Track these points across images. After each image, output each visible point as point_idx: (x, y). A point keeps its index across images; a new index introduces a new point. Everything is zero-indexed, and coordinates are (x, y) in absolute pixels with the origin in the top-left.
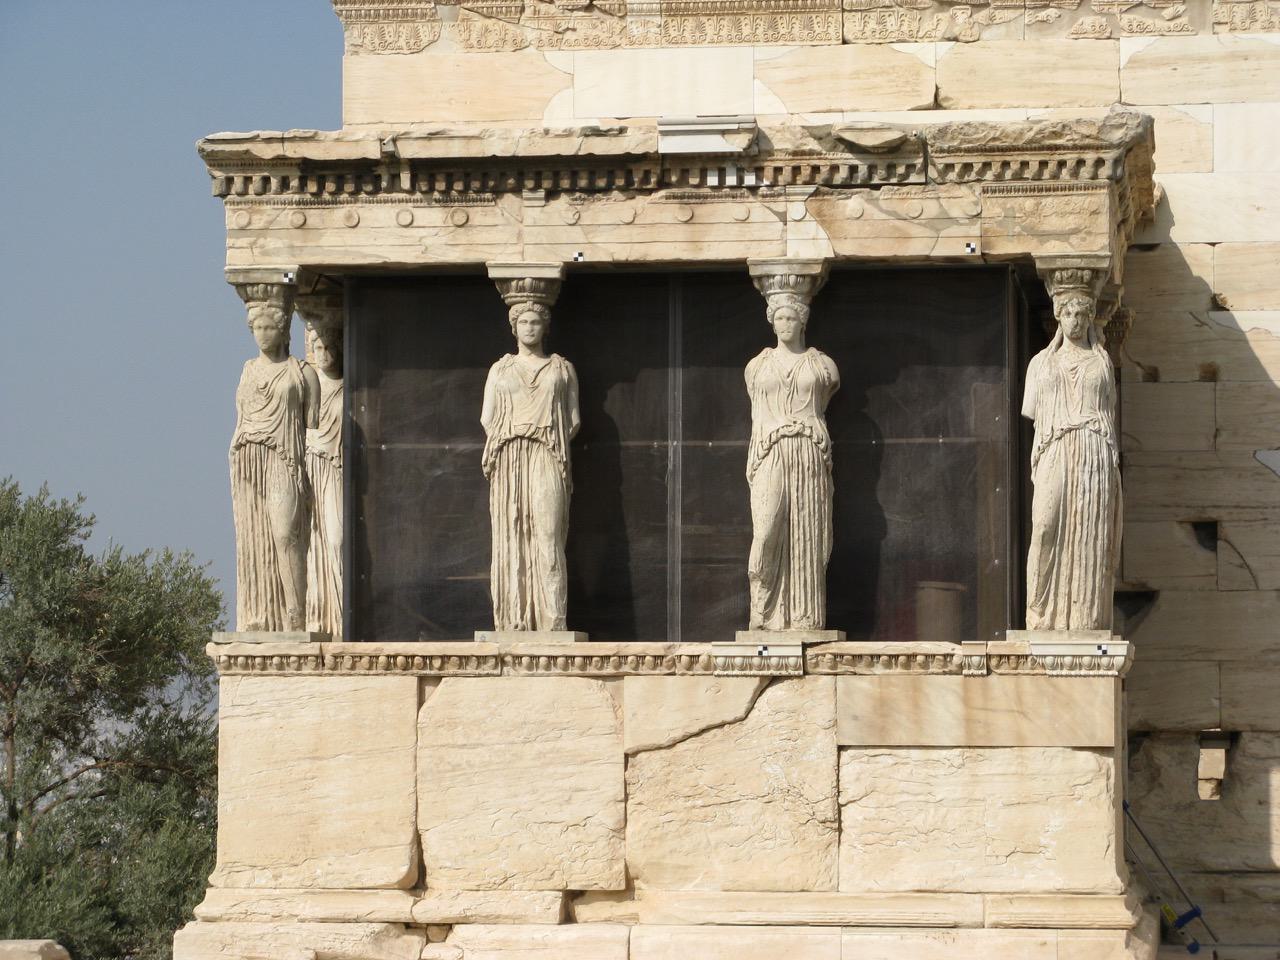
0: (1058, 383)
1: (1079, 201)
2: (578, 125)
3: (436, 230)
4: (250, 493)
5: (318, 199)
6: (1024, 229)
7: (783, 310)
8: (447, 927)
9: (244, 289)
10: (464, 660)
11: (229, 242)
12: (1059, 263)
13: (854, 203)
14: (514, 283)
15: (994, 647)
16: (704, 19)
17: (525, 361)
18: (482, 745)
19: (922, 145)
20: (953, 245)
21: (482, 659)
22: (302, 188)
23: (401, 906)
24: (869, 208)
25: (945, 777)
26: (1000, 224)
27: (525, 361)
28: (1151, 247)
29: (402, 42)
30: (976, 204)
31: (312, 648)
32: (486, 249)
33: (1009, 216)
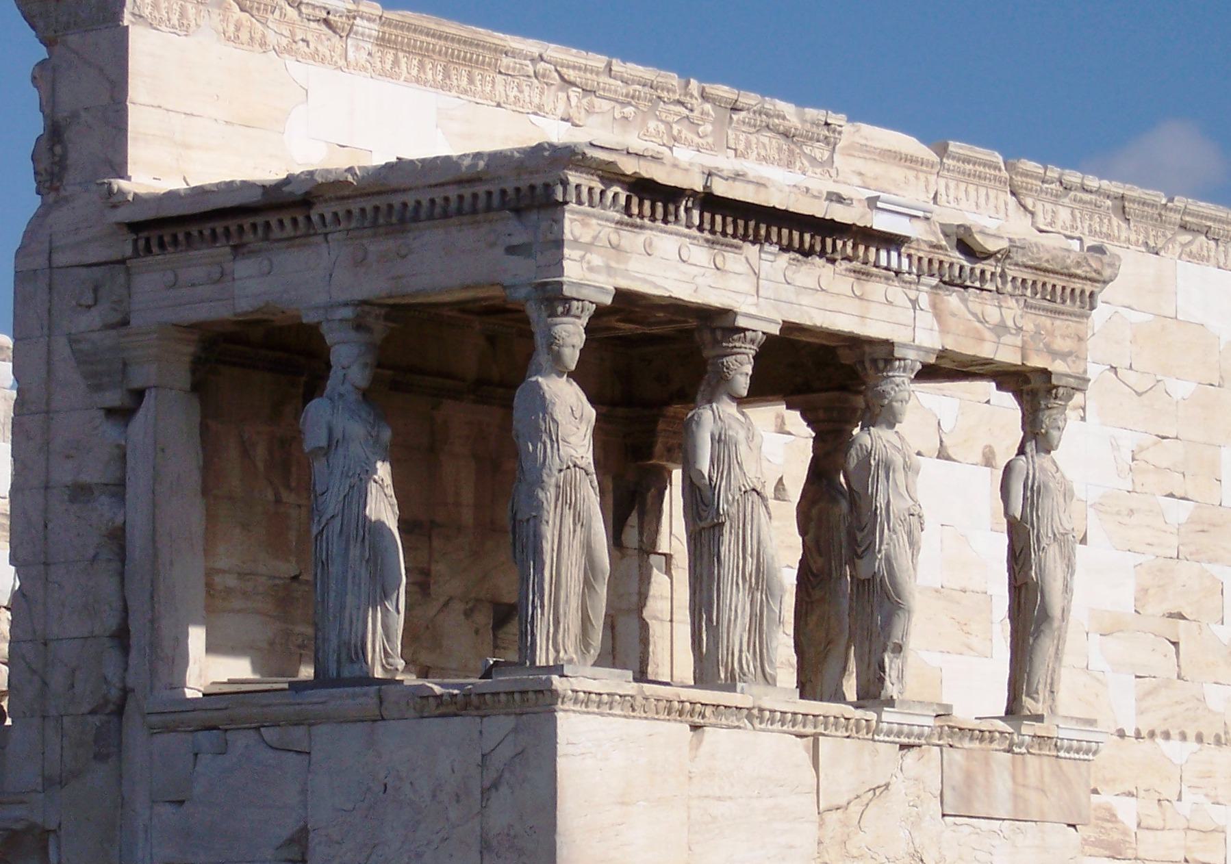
1: (1071, 325)
3: (703, 270)
6: (1047, 346)
11: (566, 251)
12: (1063, 382)
13: (953, 299)
14: (748, 334)
16: (401, 54)
18: (730, 798)
22: (627, 209)
24: (962, 306)
26: (1032, 337)
29: (175, 21)
30: (1022, 317)
32: (733, 295)
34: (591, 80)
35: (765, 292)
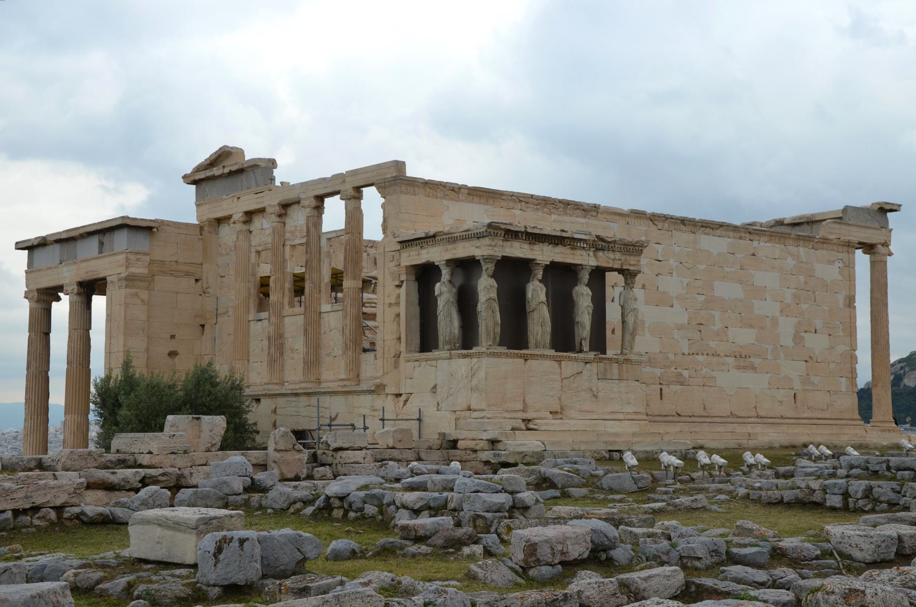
1: (636, 258)
4: (490, 312)
13: (600, 254)
34: (527, 200)
35: (544, 254)
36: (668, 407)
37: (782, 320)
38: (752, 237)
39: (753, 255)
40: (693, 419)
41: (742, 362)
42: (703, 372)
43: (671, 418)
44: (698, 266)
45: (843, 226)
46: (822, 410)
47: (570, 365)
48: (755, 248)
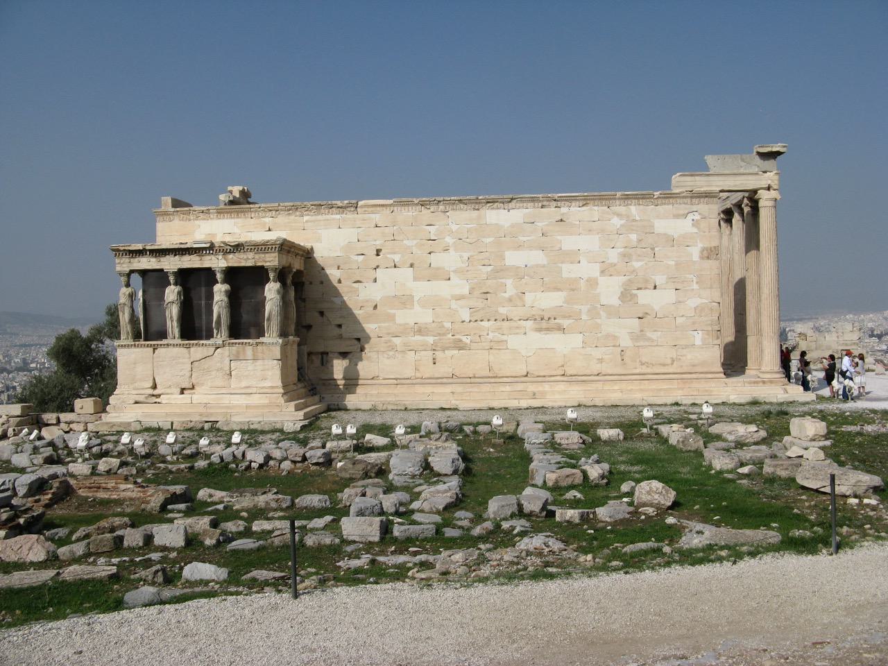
0: (270, 290)
2: (178, 242)
5: (132, 257)
7: (219, 276)
8: (159, 395)
9: (121, 274)
10: (161, 345)
13: (231, 256)
15: (258, 341)
17: (172, 287)
19: (242, 245)
20: (249, 264)
21: (164, 345)
23: (151, 391)
25: (250, 365)
27: (172, 287)
28: (310, 258)
31: (133, 343)
33: (260, 258)
36: (443, 370)
37: (603, 281)
38: (559, 204)
39: (561, 220)
40: (473, 380)
41: (544, 324)
42: (491, 336)
43: (445, 380)
44: (483, 240)
45: (697, 178)
46: (664, 365)
47: (199, 350)
48: (563, 214)
